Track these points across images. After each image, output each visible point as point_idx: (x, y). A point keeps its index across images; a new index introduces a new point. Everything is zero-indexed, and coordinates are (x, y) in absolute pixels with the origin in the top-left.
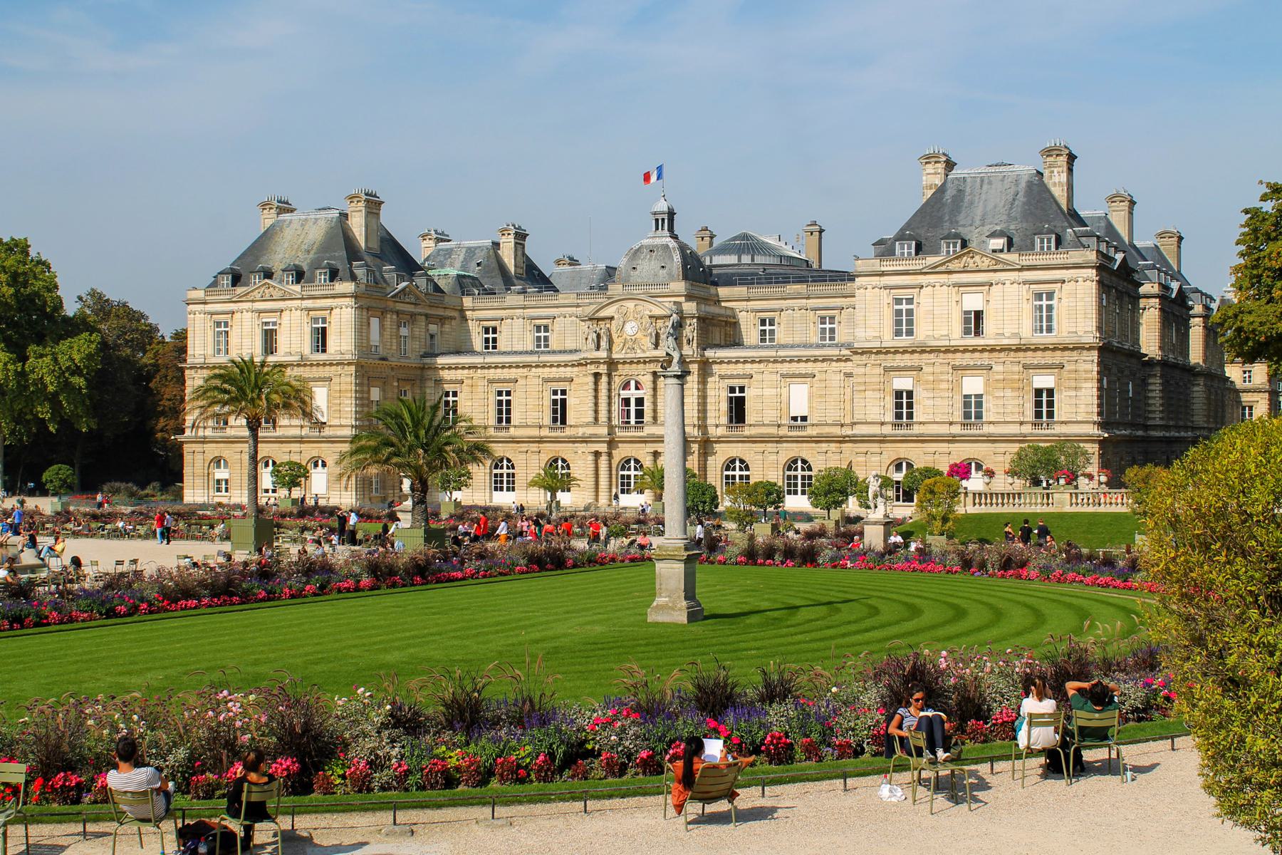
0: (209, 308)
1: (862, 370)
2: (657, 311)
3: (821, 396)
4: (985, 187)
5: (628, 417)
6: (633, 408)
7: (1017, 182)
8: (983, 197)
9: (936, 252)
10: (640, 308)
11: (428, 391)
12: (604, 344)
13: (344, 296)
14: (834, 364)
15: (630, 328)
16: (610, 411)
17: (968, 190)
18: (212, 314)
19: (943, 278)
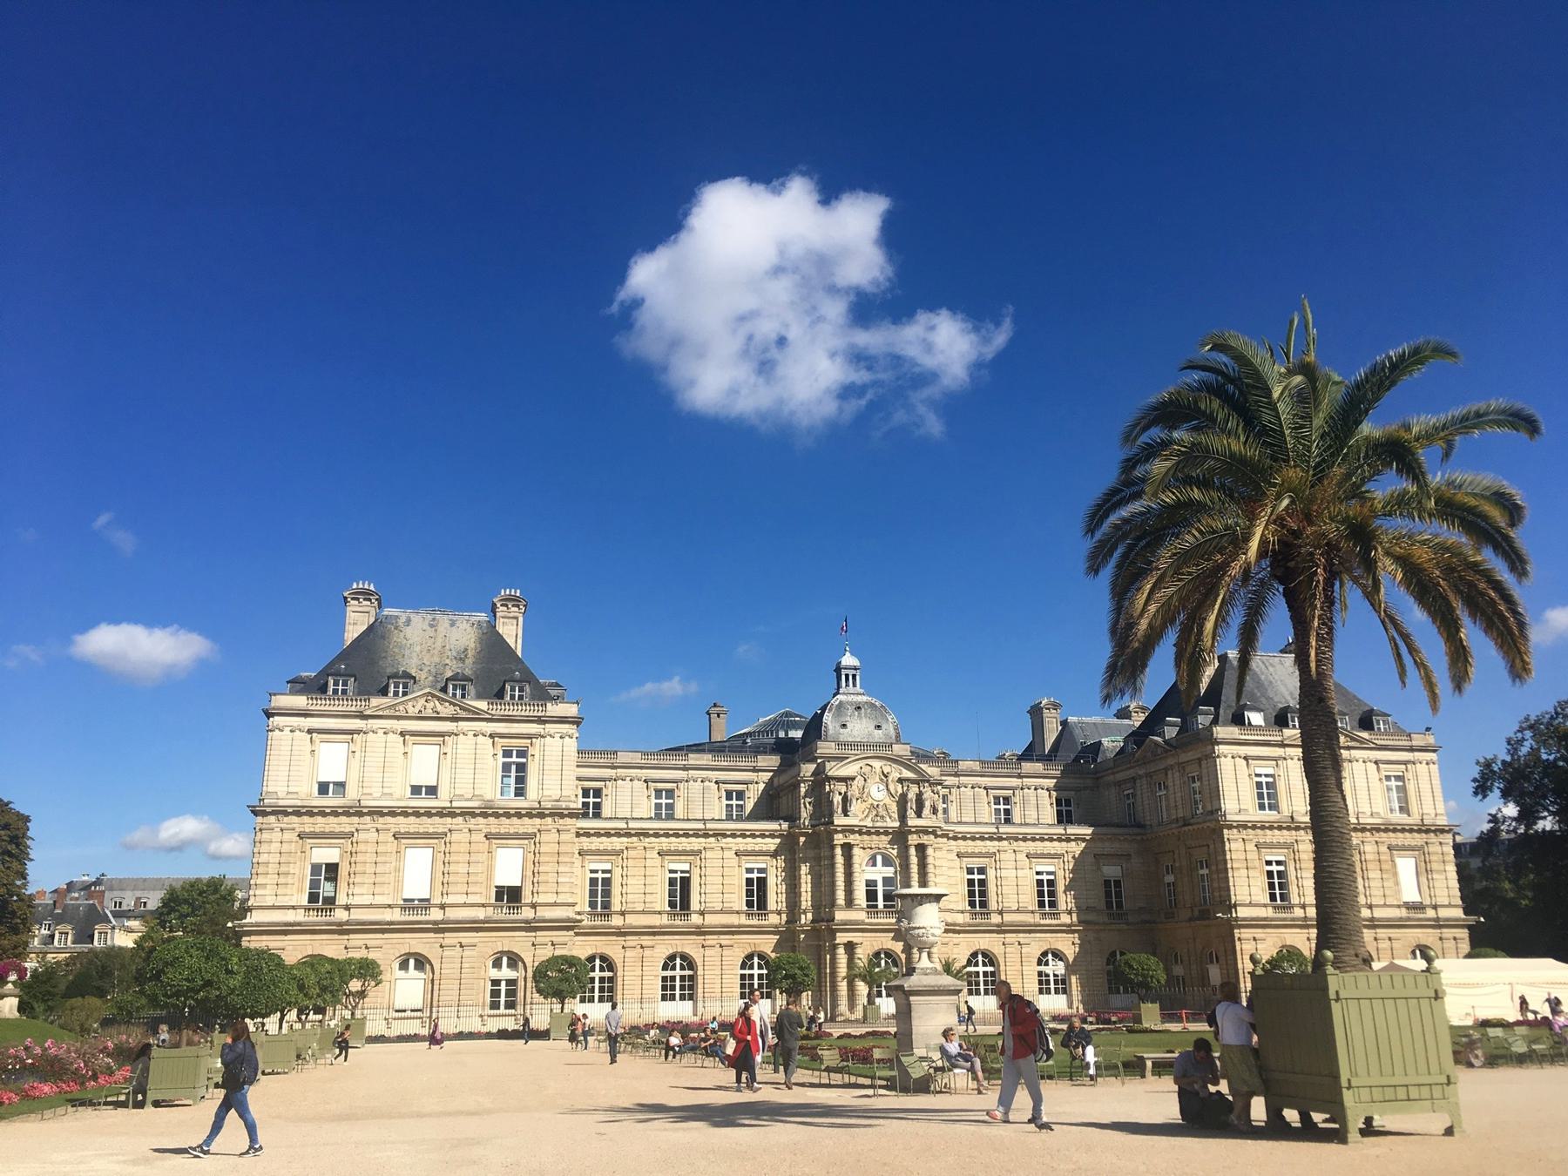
1: (1234, 846)
2: (908, 774)
9: (1287, 726)
13: (562, 720)
15: (877, 793)
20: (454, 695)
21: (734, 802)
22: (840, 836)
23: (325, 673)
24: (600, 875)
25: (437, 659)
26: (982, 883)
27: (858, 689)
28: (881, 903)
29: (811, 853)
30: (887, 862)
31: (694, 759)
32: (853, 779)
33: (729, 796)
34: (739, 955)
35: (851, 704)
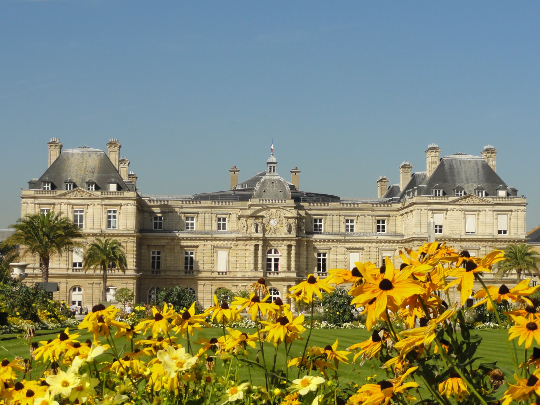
0: (37, 201)
2: (289, 214)
3: (367, 259)
4: (463, 165)
5: (271, 267)
6: (273, 263)
7: (476, 162)
8: (463, 169)
10: (279, 212)
11: (143, 251)
12: (260, 230)
14: (374, 244)
15: (273, 223)
16: (263, 265)
17: (455, 166)
18: (40, 204)
19: (458, 207)
20: (89, 189)
21: (222, 222)
22: (254, 241)
23: (42, 180)
24: (156, 255)
25: (83, 172)
26: (324, 260)
27: (276, 173)
28: (273, 269)
29: (244, 248)
30: (276, 252)
31: (204, 203)
32: (263, 217)
33: (219, 220)
34: (215, 288)
35: (269, 180)
